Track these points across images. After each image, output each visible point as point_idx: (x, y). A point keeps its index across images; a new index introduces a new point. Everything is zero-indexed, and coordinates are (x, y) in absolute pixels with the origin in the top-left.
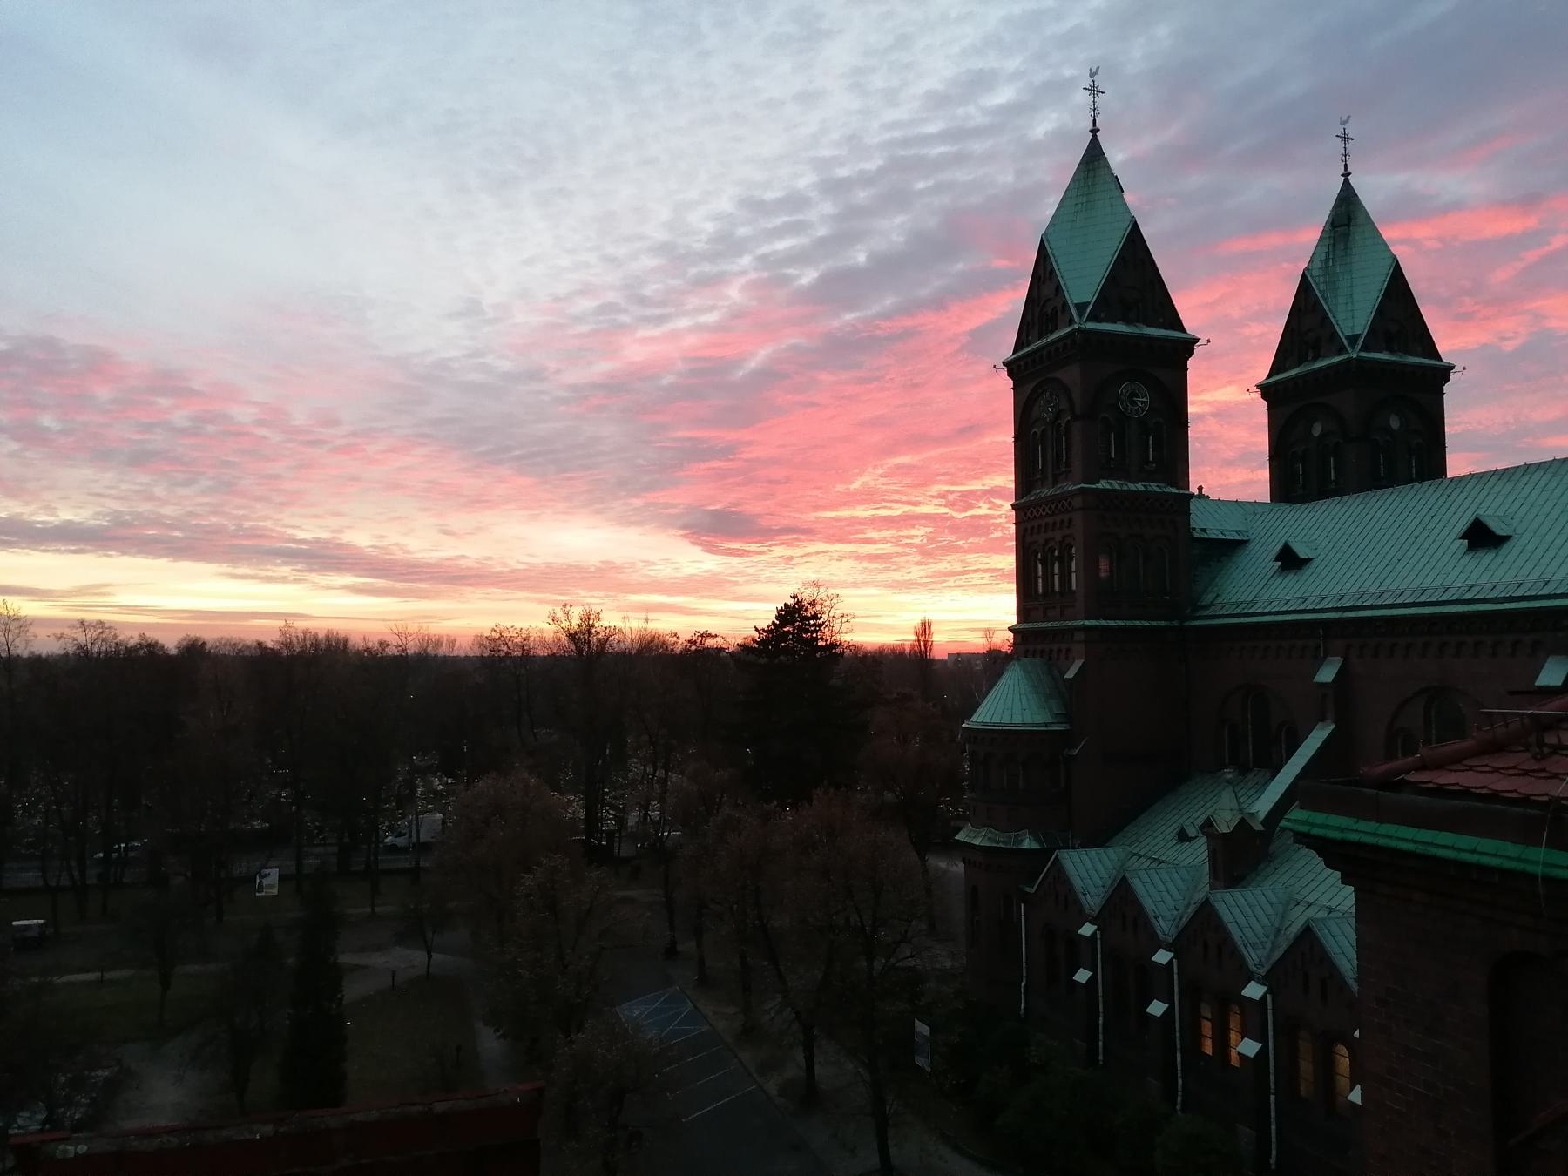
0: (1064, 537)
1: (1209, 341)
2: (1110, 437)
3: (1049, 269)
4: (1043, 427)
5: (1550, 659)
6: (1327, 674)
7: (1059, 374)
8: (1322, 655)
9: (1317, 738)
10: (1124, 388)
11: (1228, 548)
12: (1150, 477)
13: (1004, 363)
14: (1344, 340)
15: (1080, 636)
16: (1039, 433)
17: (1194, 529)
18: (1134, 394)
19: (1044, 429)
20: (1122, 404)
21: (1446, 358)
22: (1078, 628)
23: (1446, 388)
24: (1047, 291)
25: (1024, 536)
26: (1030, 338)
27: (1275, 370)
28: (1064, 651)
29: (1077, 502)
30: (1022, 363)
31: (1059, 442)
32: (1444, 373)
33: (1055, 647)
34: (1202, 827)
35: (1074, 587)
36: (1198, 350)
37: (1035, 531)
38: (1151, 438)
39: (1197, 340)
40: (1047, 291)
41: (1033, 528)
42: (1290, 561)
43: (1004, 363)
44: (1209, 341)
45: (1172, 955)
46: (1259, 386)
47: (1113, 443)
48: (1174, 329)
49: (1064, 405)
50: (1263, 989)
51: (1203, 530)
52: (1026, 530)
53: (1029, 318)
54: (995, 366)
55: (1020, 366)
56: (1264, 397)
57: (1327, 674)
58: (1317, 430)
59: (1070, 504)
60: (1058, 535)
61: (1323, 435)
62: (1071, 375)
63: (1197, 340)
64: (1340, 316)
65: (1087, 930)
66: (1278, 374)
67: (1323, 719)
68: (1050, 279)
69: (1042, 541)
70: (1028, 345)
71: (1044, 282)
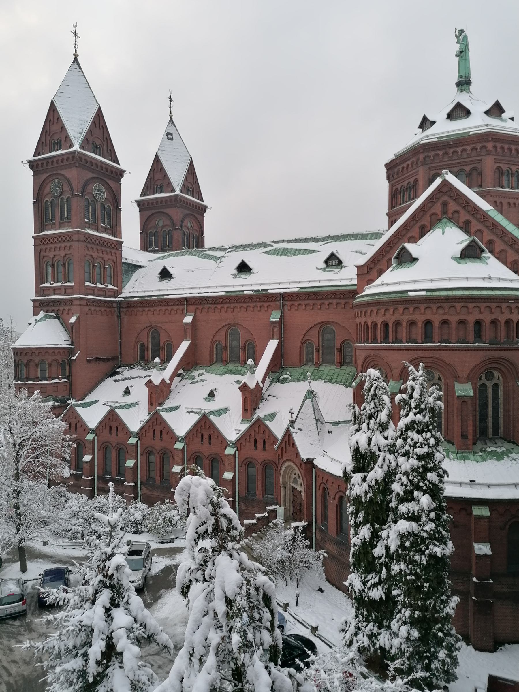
0: (66, 255)
2: (89, 208)
4: (52, 198)
5: (274, 311)
6: (188, 319)
7: (62, 172)
9: (185, 345)
10: (96, 186)
11: (136, 267)
12: (105, 230)
13: (30, 162)
15: (78, 302)
16: (50, 201)
19: (53, 199)
21: (206, 202)
22: (76, 299)
23: (205, 214)
24: (55, 128)
25: (40, 253)
26: (43, 151)
27: (143, 194)
28: (67, 310)
29: (75, 238)
30: (40, 163)
31: (62, 208)
32: (204, 209)
33: (61, 308)
34: (146, 384)
37: (48, 251)
38: (106, 212)
39: (125, 171)
40: (55, 128)
41: (46, 249)
42: (165, 274)
43: (27, 161)
45: (137, 439)
48: (114, 162)
49: (66, 188)
50: (183, 444)
51: (126, 259)
52: (41, 250)
53: (43, 140)
54: (22, 162)
55: (38, 165)
57: (188, 319)
58: (161, 224)
59: (70, 237)
60: (63, 253)
61: (164, 226)
62: (72, 173)
63: (125, 171)
65: (90, 437)
66: (144, 195)
67: (185, 338)
68: (57, 122)
69: (52, 256)
70: (42, 154)
71: (53, 123)
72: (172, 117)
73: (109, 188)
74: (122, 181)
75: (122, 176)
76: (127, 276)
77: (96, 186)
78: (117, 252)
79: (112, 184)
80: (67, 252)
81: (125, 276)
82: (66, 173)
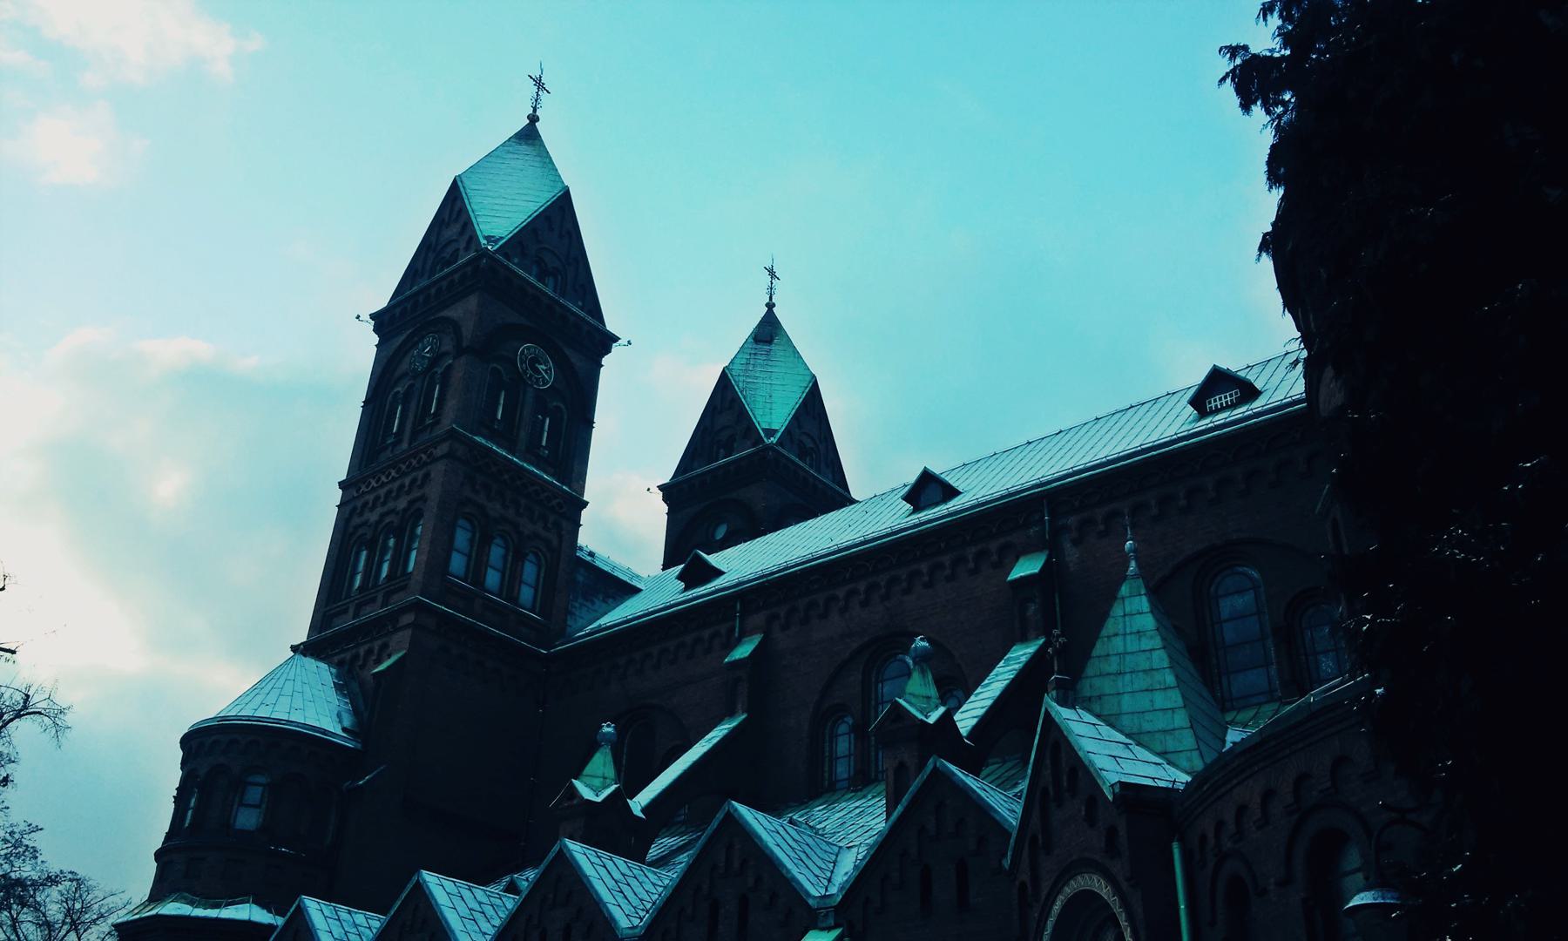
1: (629, 343)
3: (456, 209)
8: (737, 635)
14: (761, 431)
17: (581, 549)
18: (534, 361)
20: (521, 364)
24: (451, 232)
35: (411, 567)
36: (615, 348)
39: (616, 339)
44: (629, 343)
46: (661, 488)
47: (502, 402)
56: (665, 499)
60: (402, 504)
63: (616, 339)
64: (758, 412)
72: (775, 310)
73: (563, 365)
74: (605, 360)
75: (608, 351)
76: (589, 604)
77: (528, 348)
78: (565, 524)
79: (576, 359)
80: (416, 494)
81: (580, 600)
82: (455, 312)
